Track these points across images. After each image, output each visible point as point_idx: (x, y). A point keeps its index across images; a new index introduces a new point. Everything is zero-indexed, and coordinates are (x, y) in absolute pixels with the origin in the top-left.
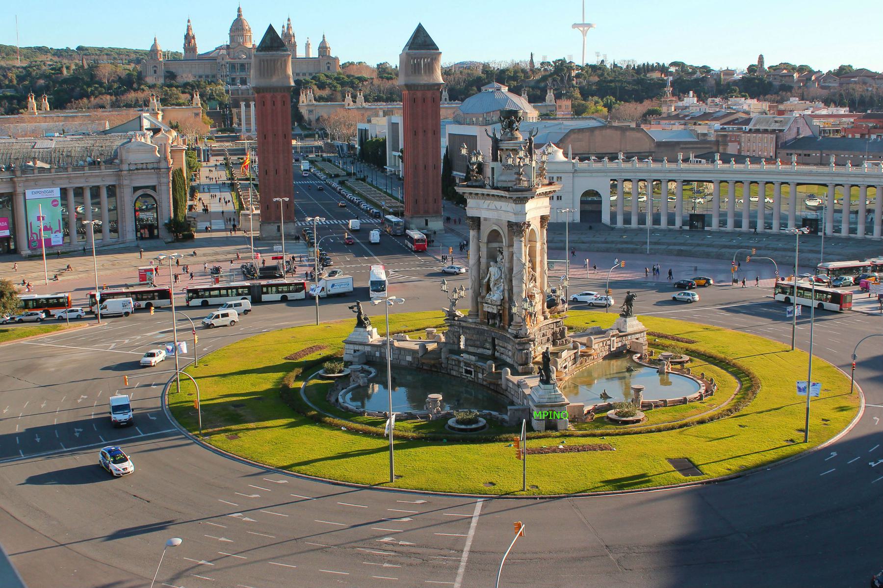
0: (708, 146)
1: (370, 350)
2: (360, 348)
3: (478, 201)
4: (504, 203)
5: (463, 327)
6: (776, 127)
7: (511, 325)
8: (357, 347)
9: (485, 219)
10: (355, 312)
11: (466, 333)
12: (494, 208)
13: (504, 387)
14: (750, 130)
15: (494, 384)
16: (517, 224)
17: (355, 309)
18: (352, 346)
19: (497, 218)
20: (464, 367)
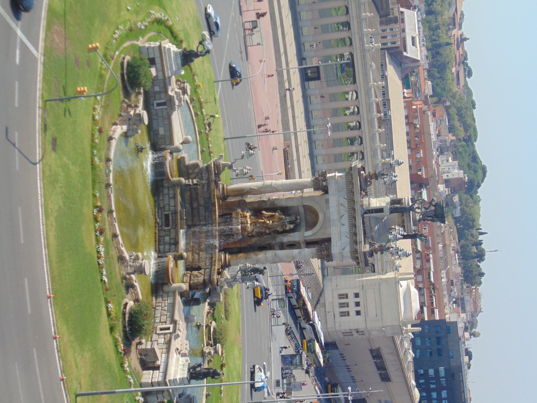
0: (384, 6)
1: (159, 78)
2: (159, 66)
3: (345, 190)
4: (348, 230)
5: (209, 184)
6: (409, 42)
7: (225, 253)
8: (158, 61)
9: (327, 201)
10: (197, 48)
11: (203, 188)
12: (341, 214)
13: (166, 288)
14: (402, 13)
15: (162, 257)
16: (329, 249)
17: (201, 49)
18: (157, 55)
19: (331, 219)
20: (170, 212)
